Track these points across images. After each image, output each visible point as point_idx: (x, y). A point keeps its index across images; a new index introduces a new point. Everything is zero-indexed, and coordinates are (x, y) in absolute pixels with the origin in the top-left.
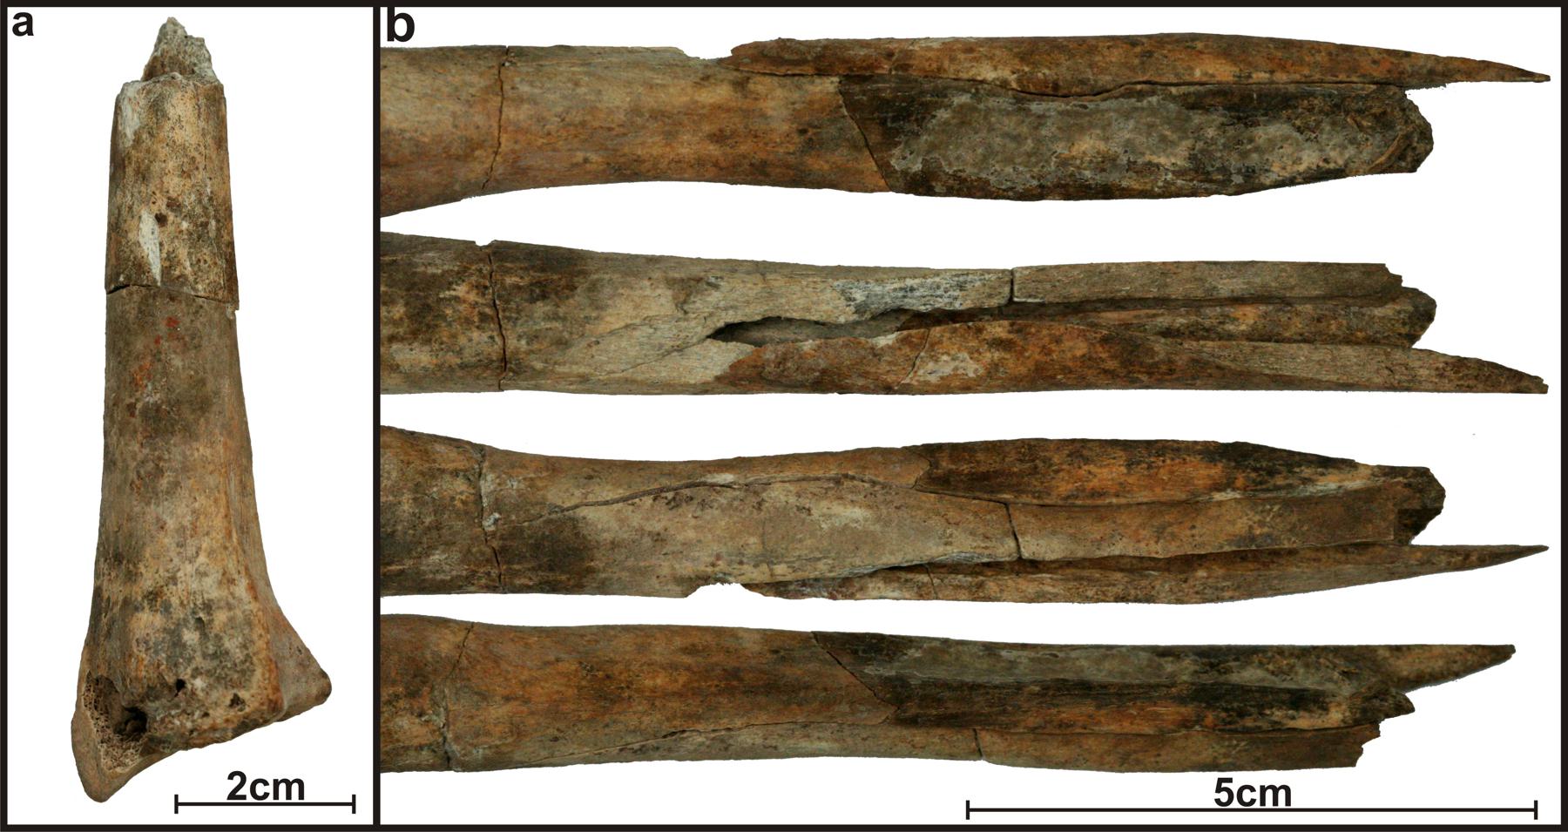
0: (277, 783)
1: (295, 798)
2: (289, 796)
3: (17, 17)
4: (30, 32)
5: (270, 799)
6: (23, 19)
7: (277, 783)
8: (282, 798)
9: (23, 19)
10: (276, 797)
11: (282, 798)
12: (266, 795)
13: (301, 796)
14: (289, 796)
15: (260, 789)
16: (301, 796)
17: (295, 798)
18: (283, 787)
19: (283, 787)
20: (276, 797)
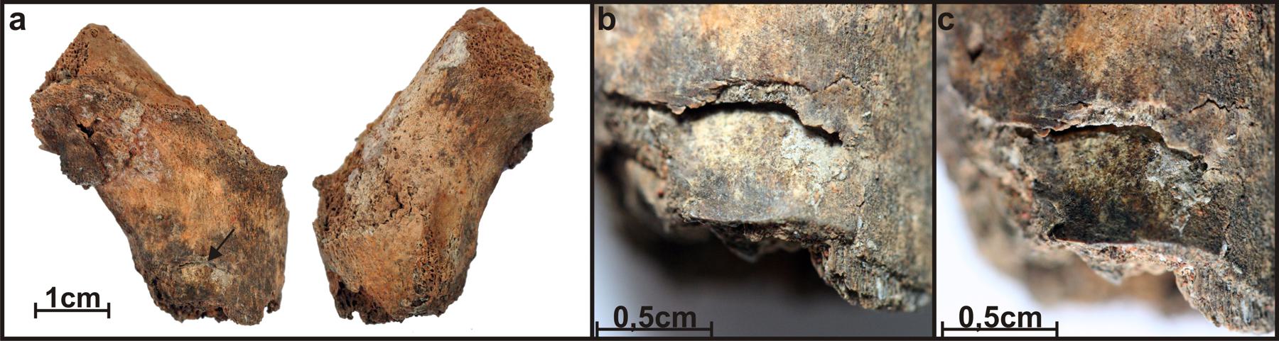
0: (80, 295)
1: (93, 306)
2: (89, 305)
3: (13, 16)
4: (22, 27)
5: (75, 307)
6: (18, 18)
7: (80, 295)
8: (84, 306)
9: (18, 18)
10: (80, 305)
11: (84, 306)
12: (73, 304)
13: (98, 305)
14: (89, 305)
15: (69, 300)
16: (98, 305)
17: (93, 306)
18: (84, 298)
19: (84, 298)
20: (80, 305)
